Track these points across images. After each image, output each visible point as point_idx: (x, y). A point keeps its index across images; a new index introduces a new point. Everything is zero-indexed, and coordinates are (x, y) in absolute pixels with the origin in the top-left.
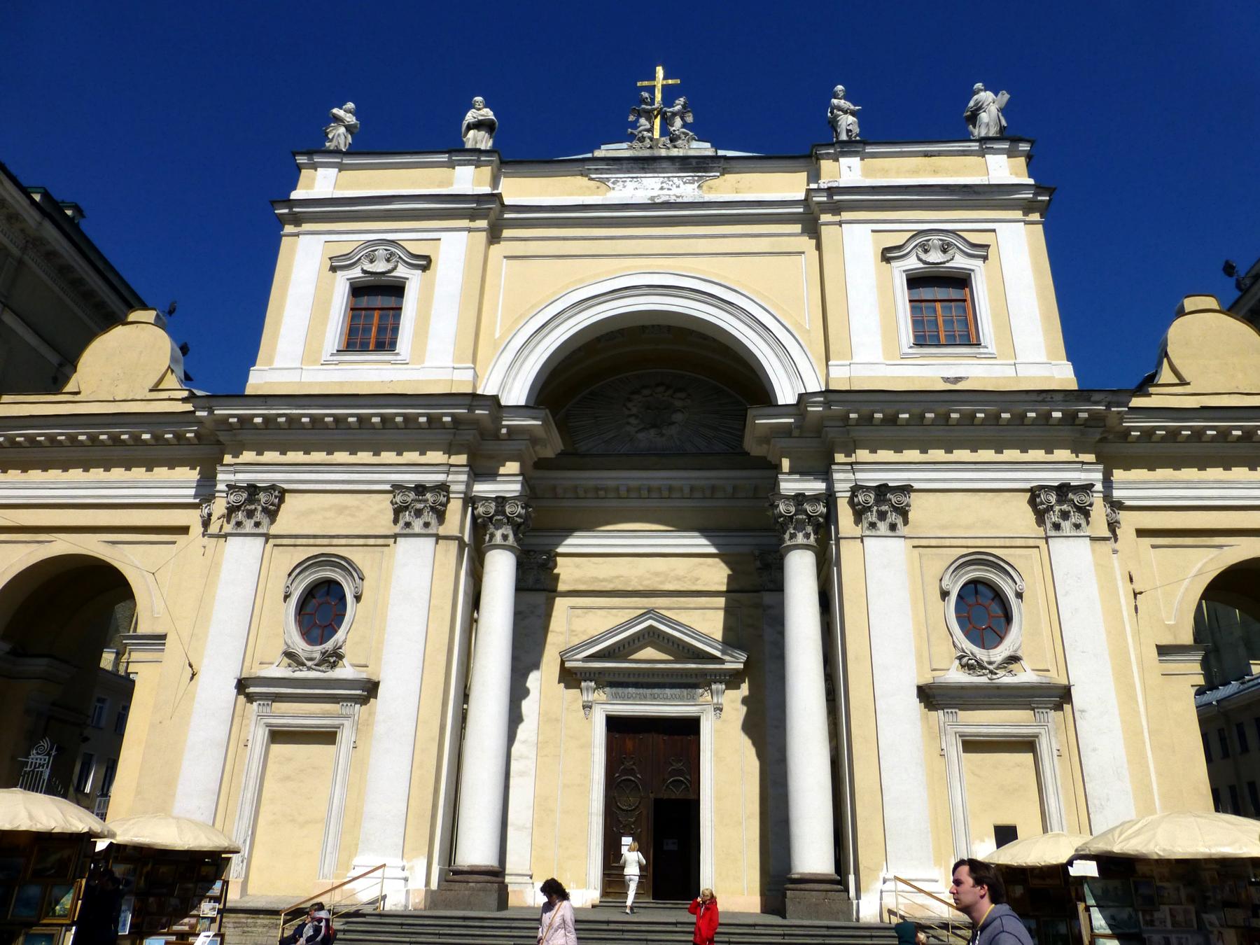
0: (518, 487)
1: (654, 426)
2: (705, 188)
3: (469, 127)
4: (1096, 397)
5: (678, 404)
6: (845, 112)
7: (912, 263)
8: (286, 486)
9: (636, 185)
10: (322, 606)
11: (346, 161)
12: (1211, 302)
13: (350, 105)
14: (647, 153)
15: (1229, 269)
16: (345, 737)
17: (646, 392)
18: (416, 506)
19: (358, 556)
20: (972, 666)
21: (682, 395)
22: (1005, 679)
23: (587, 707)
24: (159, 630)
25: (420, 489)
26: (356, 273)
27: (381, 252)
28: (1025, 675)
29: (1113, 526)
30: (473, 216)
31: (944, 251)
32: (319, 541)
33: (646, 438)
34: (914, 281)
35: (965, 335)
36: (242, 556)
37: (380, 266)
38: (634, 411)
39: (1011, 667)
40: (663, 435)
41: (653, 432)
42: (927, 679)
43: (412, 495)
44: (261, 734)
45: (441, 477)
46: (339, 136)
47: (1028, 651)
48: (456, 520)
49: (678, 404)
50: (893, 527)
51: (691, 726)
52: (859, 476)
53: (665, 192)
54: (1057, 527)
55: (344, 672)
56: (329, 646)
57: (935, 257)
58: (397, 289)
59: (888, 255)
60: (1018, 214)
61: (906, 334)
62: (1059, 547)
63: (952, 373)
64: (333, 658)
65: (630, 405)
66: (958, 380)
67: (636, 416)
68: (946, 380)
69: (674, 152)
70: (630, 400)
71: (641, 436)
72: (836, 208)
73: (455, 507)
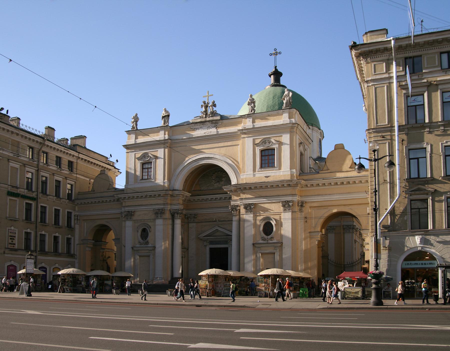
14: (203, 120)
18: (159, 213)
19: (150, 224)
25: (159, 210)
45: (163, 207)
48: (168, 215)
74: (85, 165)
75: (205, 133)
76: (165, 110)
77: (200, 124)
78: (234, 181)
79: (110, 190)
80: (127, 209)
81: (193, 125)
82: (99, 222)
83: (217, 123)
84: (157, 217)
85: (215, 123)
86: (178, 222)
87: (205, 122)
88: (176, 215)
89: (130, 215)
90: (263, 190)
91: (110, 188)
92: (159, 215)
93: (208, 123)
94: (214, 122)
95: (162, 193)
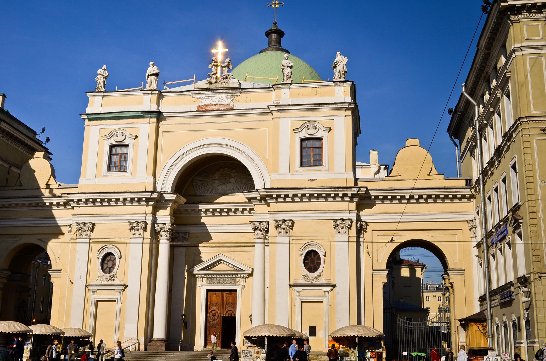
0: (169, 219)
1: (224, 184)
2: (234, 101)
3: (149, 76)
5: (233, 175)
6: (288, 67)
8: (94, 222)
9: (210, 100)
10: (108, 261)
11: (105, 94)
12: (416, 142)
13: (104, 67)
16: (119, 301)
17: (221, 170)
21: (234, 171)
24: (59, 268)
26: (112, 142)
28: (323, 281)
35: (319, 163)
36: (82, 246)
39: (319, 278)
41: (223, 186)
43: (135, 224)
46: (100, 81)
47: (324, 273)
51: (235, 291)
55: (117, 282)
56: (112, 274)
57: (312, 131)
60: (342, 112)
62: (338, 239)
64: (113, 278)
65: (215, 175)
66: (313, 180)
67: (217, 180)
68: (310, 180)
69: (224, 85)
70: (215, 173)
71: (219, 188)
73: (149, 227)
74: (6, 141)
77: (208, 92)
82: (25, 240)
83: (235, 93)
85: (232, 93)
87: (217, 89)
88: (163, 234)
94: (230, 91)
95: (144, 196)
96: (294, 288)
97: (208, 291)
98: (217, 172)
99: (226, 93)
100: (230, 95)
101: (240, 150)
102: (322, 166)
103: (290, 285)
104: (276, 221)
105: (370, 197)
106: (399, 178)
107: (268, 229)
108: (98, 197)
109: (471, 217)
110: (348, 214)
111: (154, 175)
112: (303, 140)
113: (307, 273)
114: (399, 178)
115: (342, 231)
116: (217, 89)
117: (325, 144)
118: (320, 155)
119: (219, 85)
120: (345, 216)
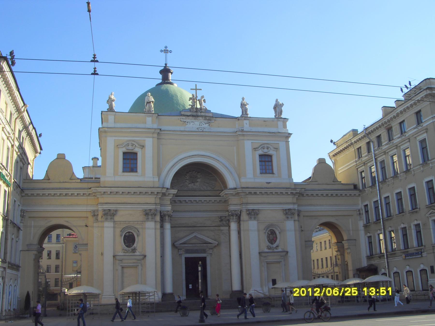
1: (193, 182)
4: (297, 190)
7: (260, 152)
14: (195, 114)
15: (332, 141)
17: (190, 173)
18: (148, 214)
20: (269, 248)
21: (200, 174)
22: (276, 251)
23: (181, 255)
24: (85, 242)
26: (124, 150)
27: (130, 144)
29: (299, 215)
30: (153, 133)
31: (268, 148)
32: (126, 222)
33: (191, 186)
34: (260, 156)
37: (130, 147)
38: (188, 178)
40: (195, 185)
41: (193, 184)
42: (261, 251)
44: (120, 268)
45: (154, 207)
49: (199, 176)
50: (255, 218)
52: (248, 206)
53: (200, 126)
54: (288, 218)
56: (133, 247)
57: (266, 150)
58: (136, 154)
59: (255, 149)
61: (258, 171)
63: (268, 181)
64: (134, 250)
65: (186, 176)
66: (269, 183)
68: (267, 183)
69: (202, 114)
70: (186, 175)
71: (189, 185)
72: (243, 135)
75: (198, 129)
76: (278, 107)
78: (231, 183)
79: (74, 181)
80: (106, 207)
81: (184, 117)
84: (148, 219)
85: (209, 120)
86: (168, 226)
88: (167, 218)
89: (110, 214)
90: (323, 198)
91: (72, 178)
92: (150, 217)
93: (201, 118)
94: (208, 118)
96: (263, 254)
97: (186, 258)
98: (187, 174)
99: (205, 119)
100: (206, 121)
101: (218, 161)
102: (273, 173)
103: (259, 253)
104: (248, 210)
105: (303, 195)
106: (317, 183)
107: (240, 215)
108: (120, 190)
109: (359, 207)
110: (292, 206)
111: (159, 175)
112: (260, 156)
113: (270, 245)
114: (317, 183)
115: (290, 217)
116: (198, 116)
117: (274, 159)
118: (272, 165)
119: (199, 114)
120: (291, 207)
